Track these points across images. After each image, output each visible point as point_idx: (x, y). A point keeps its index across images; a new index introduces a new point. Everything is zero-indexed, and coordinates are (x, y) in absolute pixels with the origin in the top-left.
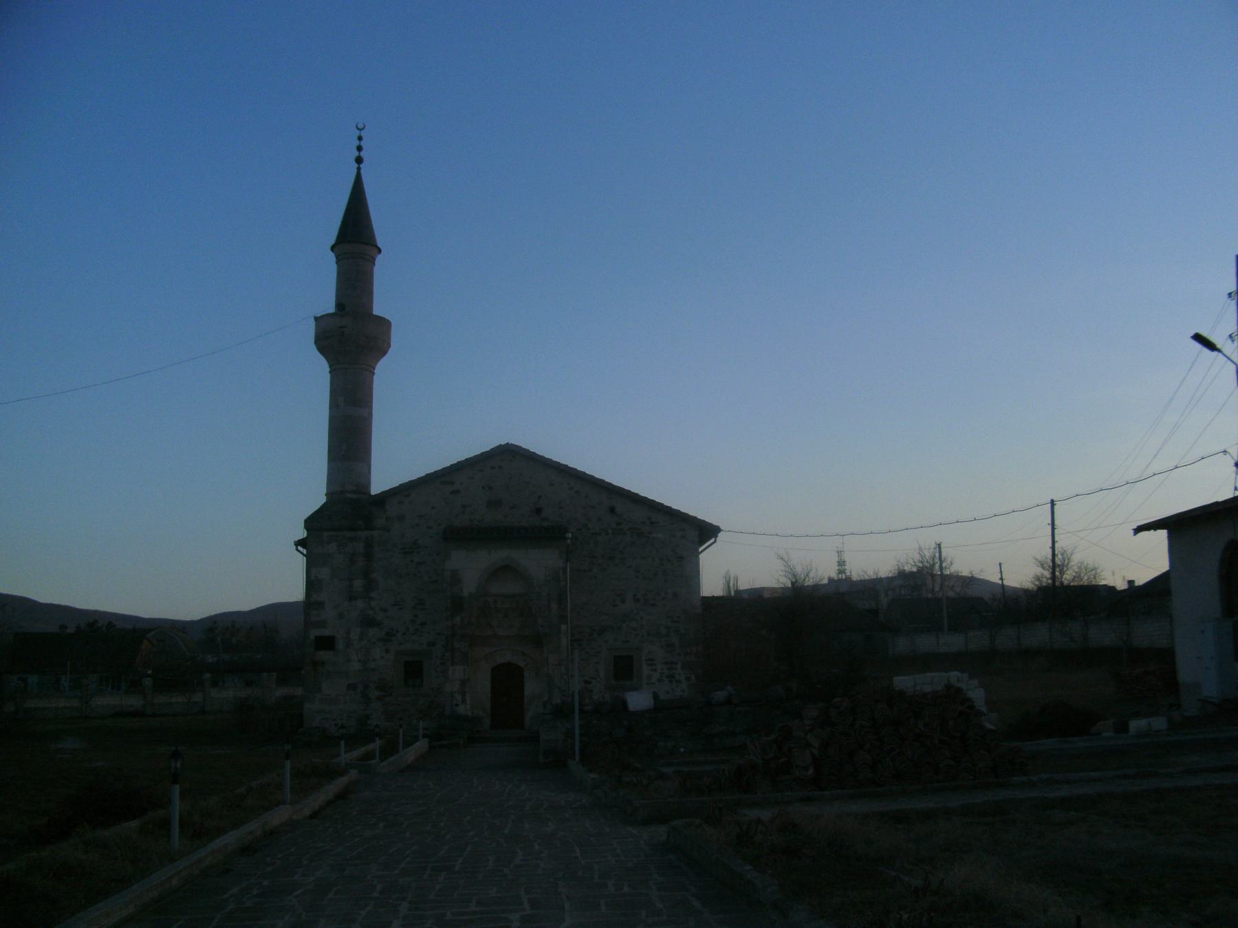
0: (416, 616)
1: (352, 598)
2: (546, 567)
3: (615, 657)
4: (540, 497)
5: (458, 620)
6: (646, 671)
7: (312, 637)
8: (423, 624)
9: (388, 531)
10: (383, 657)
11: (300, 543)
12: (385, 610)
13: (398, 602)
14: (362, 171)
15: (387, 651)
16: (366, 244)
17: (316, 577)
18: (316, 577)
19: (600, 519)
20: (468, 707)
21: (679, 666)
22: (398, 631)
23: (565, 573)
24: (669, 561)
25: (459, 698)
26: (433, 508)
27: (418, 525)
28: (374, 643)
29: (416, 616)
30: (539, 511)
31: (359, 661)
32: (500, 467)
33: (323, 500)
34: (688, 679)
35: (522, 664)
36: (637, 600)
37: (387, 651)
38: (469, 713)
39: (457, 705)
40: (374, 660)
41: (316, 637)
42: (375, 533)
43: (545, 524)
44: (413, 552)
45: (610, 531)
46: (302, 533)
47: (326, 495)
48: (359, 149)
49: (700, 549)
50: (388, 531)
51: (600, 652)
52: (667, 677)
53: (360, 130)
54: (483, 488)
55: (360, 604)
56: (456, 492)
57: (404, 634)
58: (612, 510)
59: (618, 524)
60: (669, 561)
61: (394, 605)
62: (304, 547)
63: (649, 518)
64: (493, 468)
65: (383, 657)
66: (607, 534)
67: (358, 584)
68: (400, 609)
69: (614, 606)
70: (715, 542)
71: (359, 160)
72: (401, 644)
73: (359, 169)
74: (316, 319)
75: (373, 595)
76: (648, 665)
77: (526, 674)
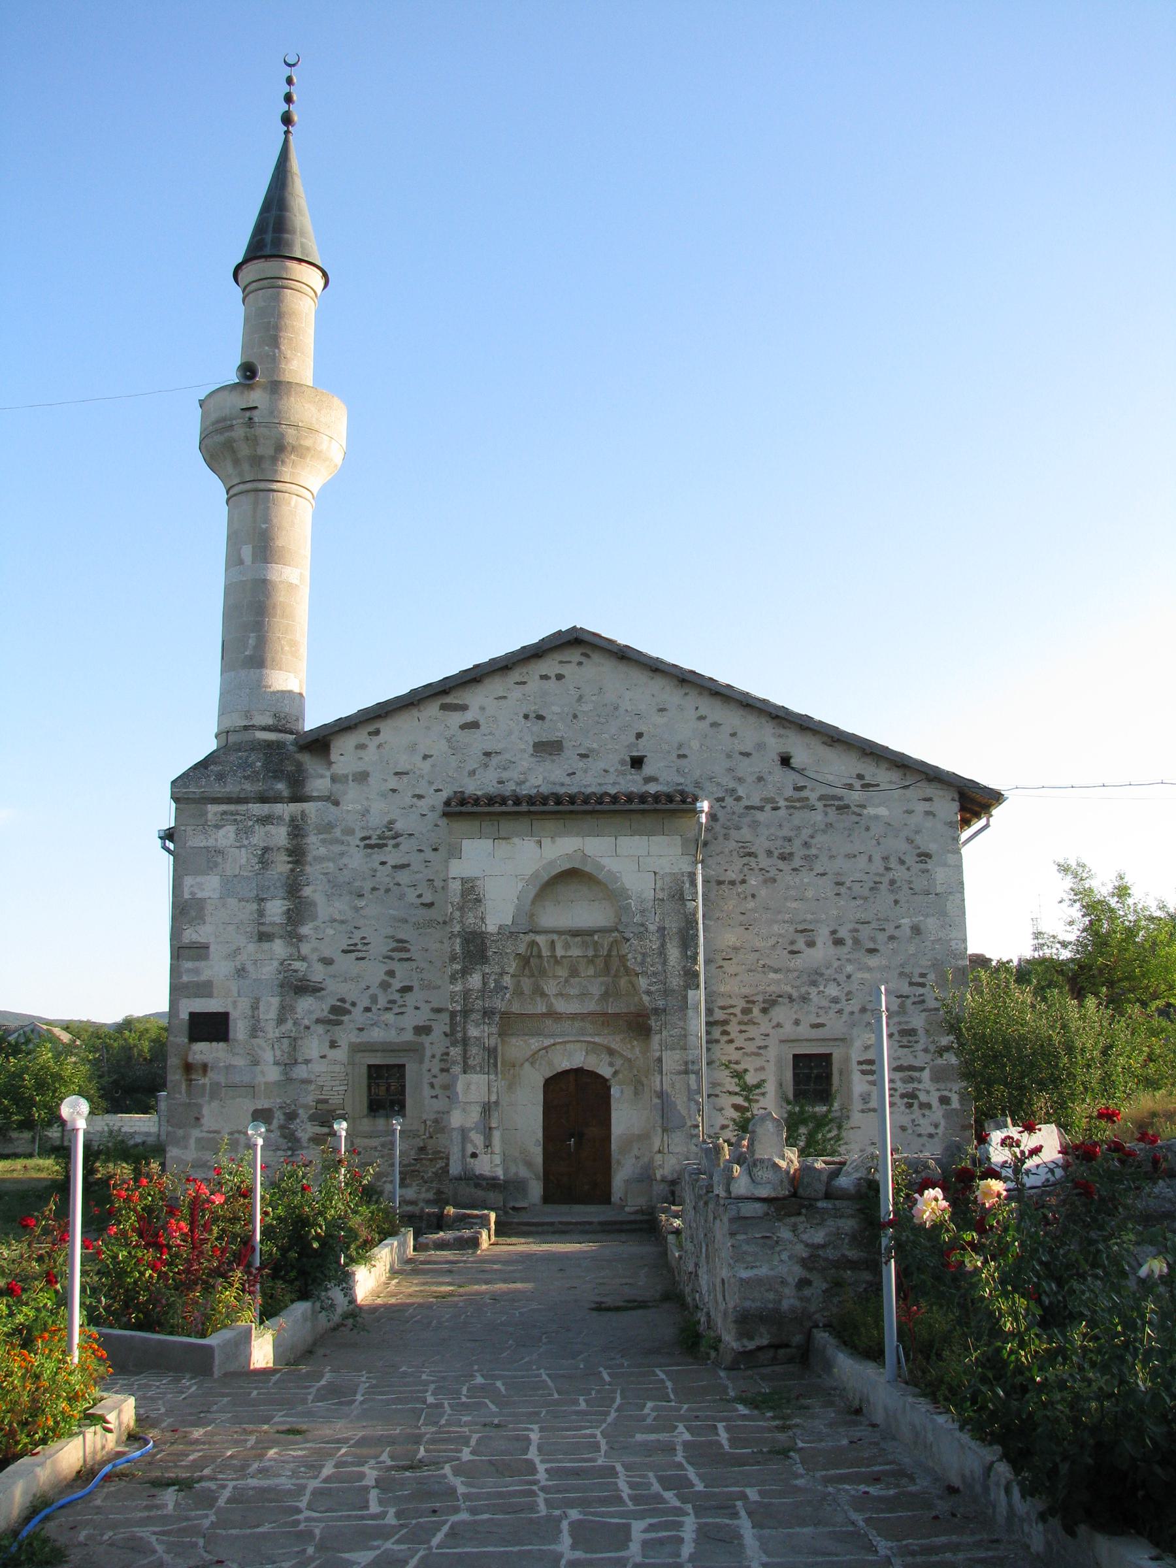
0: (391, 973)
1: (264, 937)
2: (655, 873)
3: (795, 1056)
4: (639, 735)
5: (475, 981)
6: (859, 1084)
7: (184, 1016)
8: (406, 989)
9: (336, 803)
10: (323, 1057)
11: (169, 835)
12: (327, 962)
13: (356, 945)
14: (291, 138)
15: (333, 1045)
16: (300, 260)
17: (192, 893)
18: (192, 893)
19: (760, 779)
20: (497, 1160)
21: (926, 1075)
22: (354, 1004)
23: (693, 883)
24: (902, 862)
25: (477, 1139)
26: (425, 757)
27: (394, 791)
28: (308, 1028)
29: (391, 973)
30: (637, 762)
31: (276, 1063)
32: (560, 677)
33: (211, 745)
34: (944, 1100)
35: (605, 1071)
36: (839, 942)
37: (333, 1045)
38: (500, 1173)
39: (474, 1155)
40: (307, 1062)
41: (192, 1015)
42: (309, 807)
43: (652, 788)
44: (386, 845)
45: (782, 803)
46: (166, 815)
47: (217, 736)
48: (288, 99)
49: (965, 835)
50: (336, 803)
51: (766, 1047)
52: (903, 1096)
53: (290, 65)
54: (526, 717)
55: (279, 948)
56: (474, 725)
57: (368, 1009)
58: (785, 761)
59: (798, 789)
60: (902, 862)
61: (344, 951)
62: (172, 840)
63: (860, 777)
64: (545, 677)
65: (323, 1057)
66: (775, 809)
67: (276, 909)
68: (357, 959)
69: (793, 952)
70: (987, 826)
71: (287, 120)
72: (361, 1030)
73: (287, 133)
74: (202, 403)
75: (305, 930)
76: (864, 1072)
77: (615, 1091)
